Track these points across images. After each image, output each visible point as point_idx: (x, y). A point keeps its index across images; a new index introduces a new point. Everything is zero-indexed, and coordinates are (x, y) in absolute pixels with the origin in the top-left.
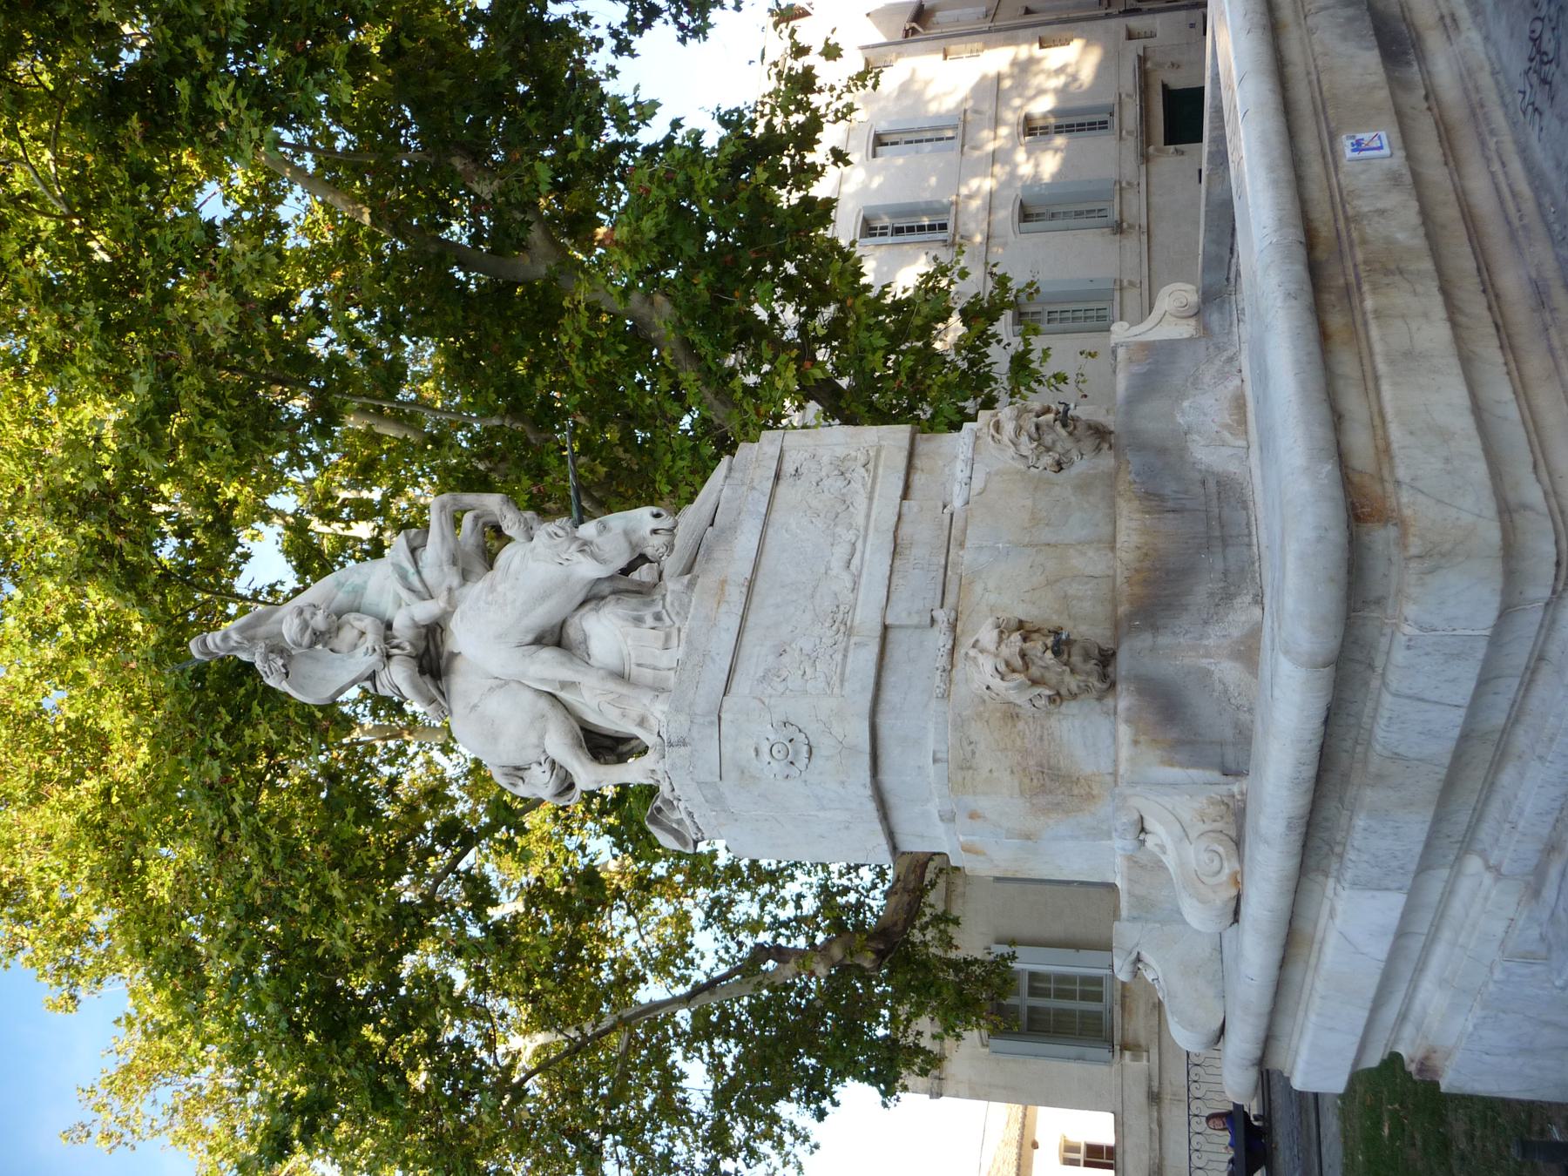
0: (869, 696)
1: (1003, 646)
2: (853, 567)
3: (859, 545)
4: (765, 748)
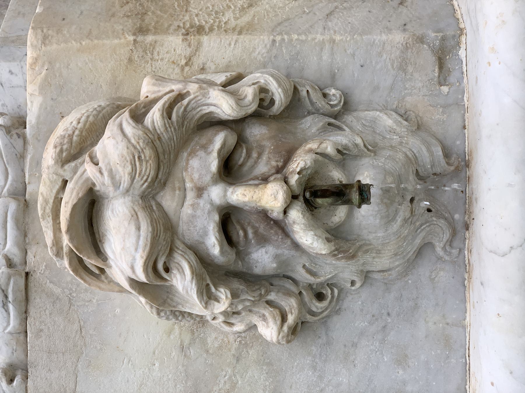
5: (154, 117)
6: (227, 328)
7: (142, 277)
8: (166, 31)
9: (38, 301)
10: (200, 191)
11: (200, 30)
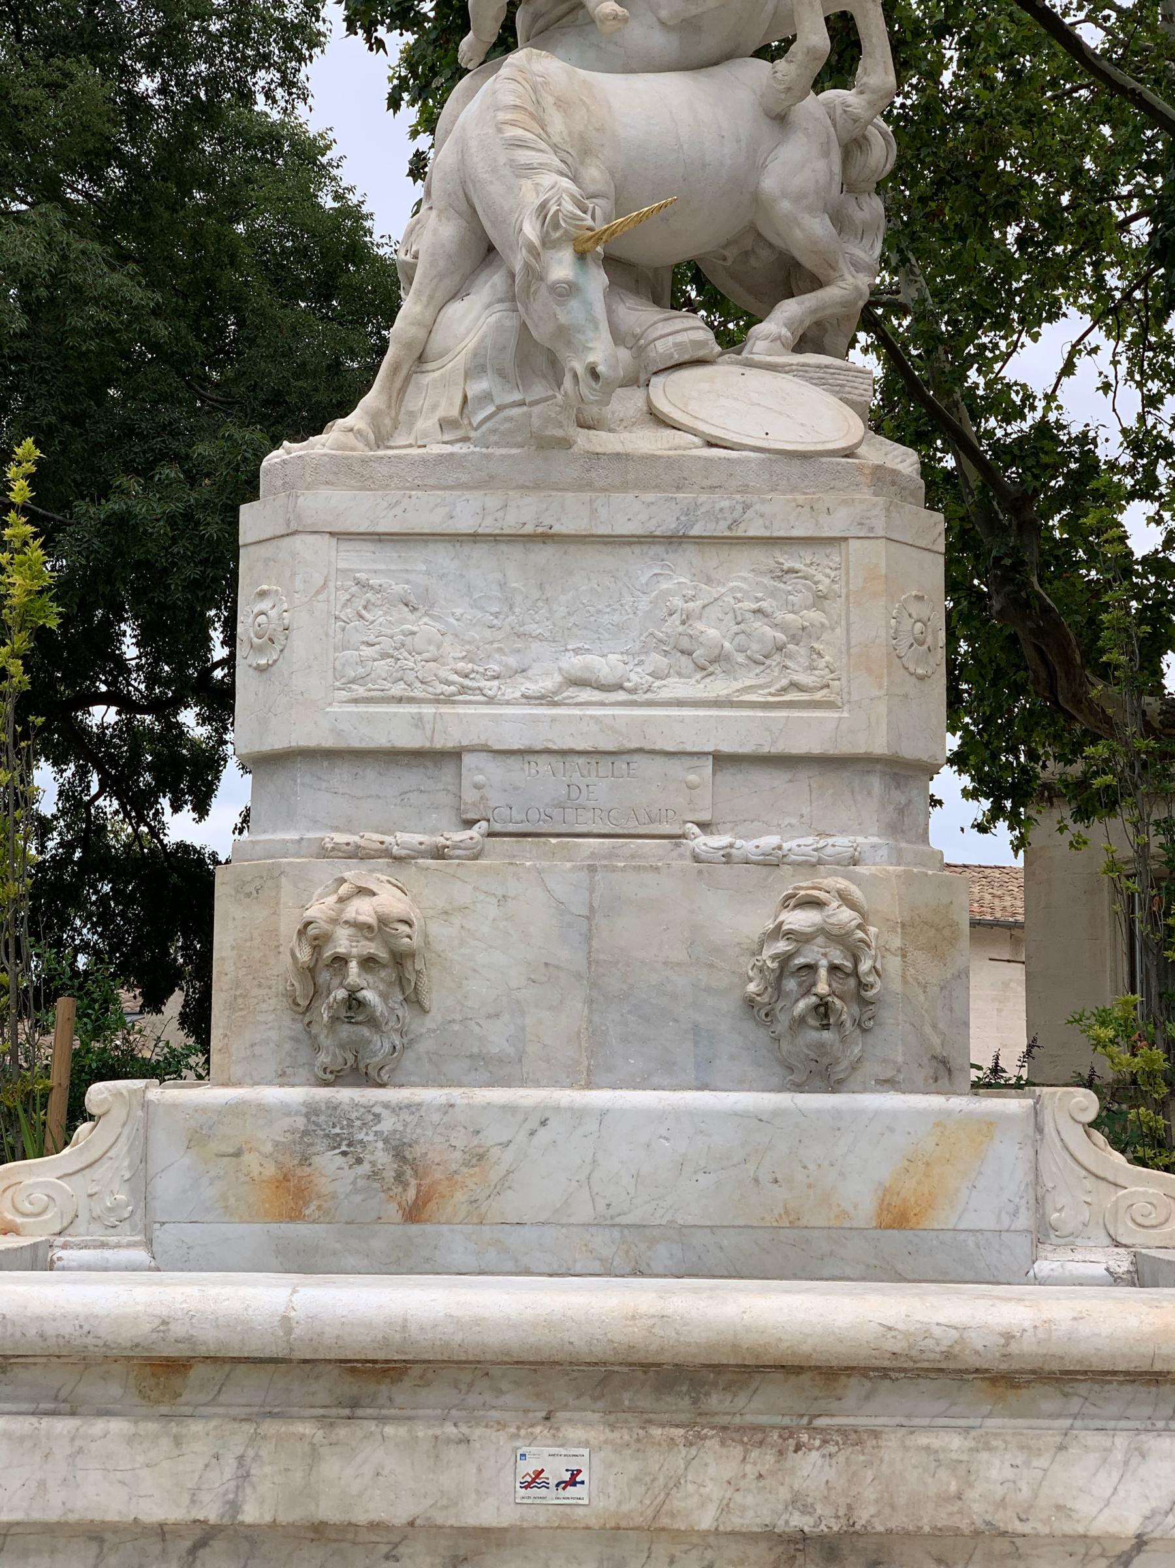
0: (329, 742)
1: (351, 931)
2: (571, 691)
3: (621, 696)
4: (265, 605)
5: (860, 934)
6: (750, 967)
7: (785, 927)
8: (902, 938)
9: (765, 870)
10: (825, 955)
11: (904, 956)
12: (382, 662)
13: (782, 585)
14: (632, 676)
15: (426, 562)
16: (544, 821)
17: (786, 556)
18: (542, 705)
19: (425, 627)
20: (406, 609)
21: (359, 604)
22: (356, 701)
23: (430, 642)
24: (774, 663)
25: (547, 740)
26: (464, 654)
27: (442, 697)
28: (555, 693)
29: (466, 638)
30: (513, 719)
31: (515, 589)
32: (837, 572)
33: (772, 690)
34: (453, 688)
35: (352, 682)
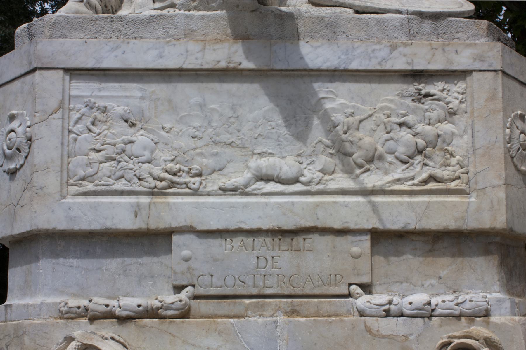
3: (298, 187)
12: (107, 164)
13: (420, 105)
14: (306, 172)
15: (141, 90)
16: (239, 286)
17: (423, 85)
18: (235, 195)
19: (142, 139)
20: (126, 124)
21: (88, 121)
22: (86, 194)
23: (145, 148)
24: (416, 162)
25: (240, 222)
26: (173, 157)
27: (156, 190)
28: (246, 186)
29: (175, 145)
30: (213, 206)
31: (213, 109)
32: (464, 96)
33: (416, 181)
34: (164, 183)
35: (83, 179)
